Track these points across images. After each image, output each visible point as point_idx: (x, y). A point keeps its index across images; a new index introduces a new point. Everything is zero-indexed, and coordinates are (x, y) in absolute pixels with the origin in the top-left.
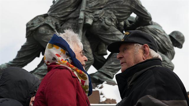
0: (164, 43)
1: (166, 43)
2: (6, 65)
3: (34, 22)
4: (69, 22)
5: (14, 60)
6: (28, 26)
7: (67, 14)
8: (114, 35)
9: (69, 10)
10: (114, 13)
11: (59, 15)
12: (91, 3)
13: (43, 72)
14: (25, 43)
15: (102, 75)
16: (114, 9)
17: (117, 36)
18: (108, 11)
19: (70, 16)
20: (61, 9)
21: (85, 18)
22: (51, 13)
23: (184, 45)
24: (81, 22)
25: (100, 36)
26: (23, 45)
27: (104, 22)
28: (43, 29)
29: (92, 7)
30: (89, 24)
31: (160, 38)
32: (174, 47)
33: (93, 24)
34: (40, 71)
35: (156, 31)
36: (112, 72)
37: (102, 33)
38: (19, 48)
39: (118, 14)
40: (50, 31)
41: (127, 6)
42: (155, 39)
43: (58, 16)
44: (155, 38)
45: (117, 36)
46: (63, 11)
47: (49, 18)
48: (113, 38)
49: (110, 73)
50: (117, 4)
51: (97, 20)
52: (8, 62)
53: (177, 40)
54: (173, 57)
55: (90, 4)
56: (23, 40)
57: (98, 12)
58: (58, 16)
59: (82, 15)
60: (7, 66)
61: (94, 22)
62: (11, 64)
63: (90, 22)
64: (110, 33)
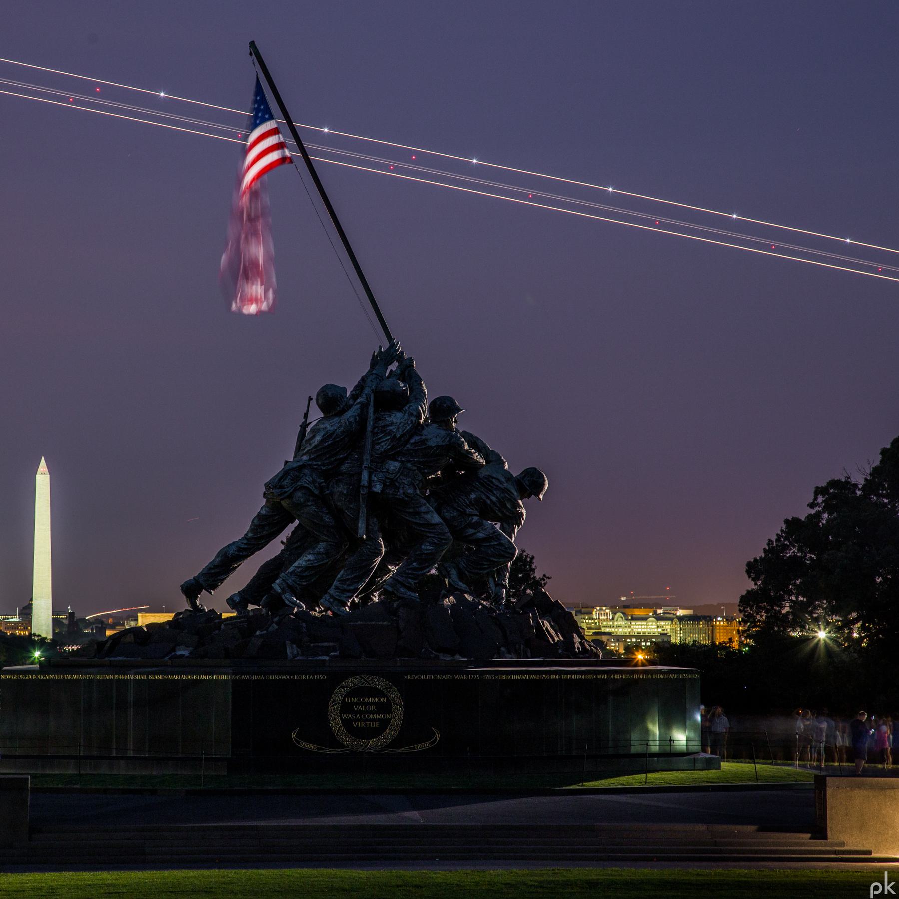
2: (234, 548)
3: (285, 483)
8: (419, 514)
10: (419, 469)
11: (324, 466)
12: (379, 443)
13: (305, 572)
15: (398, 586)
17: (423, 515)
18: (409, 465)
19: (344, 468)
21: (370, 481)
22: (310, 460)
24: (363, 492)
27: (401, 491)
28: (299, 494)
29: (381, 454)
31: (497, 498)
35: (492, 483)
42: (489, 502)
44: (488, 498)
45: (423, 515)
51: (390, 483)
55: (377, 447)
57: (393, 466)
59: (365, 475)
61: (385, 486)
62: (243, 546)
63: (378, 488)
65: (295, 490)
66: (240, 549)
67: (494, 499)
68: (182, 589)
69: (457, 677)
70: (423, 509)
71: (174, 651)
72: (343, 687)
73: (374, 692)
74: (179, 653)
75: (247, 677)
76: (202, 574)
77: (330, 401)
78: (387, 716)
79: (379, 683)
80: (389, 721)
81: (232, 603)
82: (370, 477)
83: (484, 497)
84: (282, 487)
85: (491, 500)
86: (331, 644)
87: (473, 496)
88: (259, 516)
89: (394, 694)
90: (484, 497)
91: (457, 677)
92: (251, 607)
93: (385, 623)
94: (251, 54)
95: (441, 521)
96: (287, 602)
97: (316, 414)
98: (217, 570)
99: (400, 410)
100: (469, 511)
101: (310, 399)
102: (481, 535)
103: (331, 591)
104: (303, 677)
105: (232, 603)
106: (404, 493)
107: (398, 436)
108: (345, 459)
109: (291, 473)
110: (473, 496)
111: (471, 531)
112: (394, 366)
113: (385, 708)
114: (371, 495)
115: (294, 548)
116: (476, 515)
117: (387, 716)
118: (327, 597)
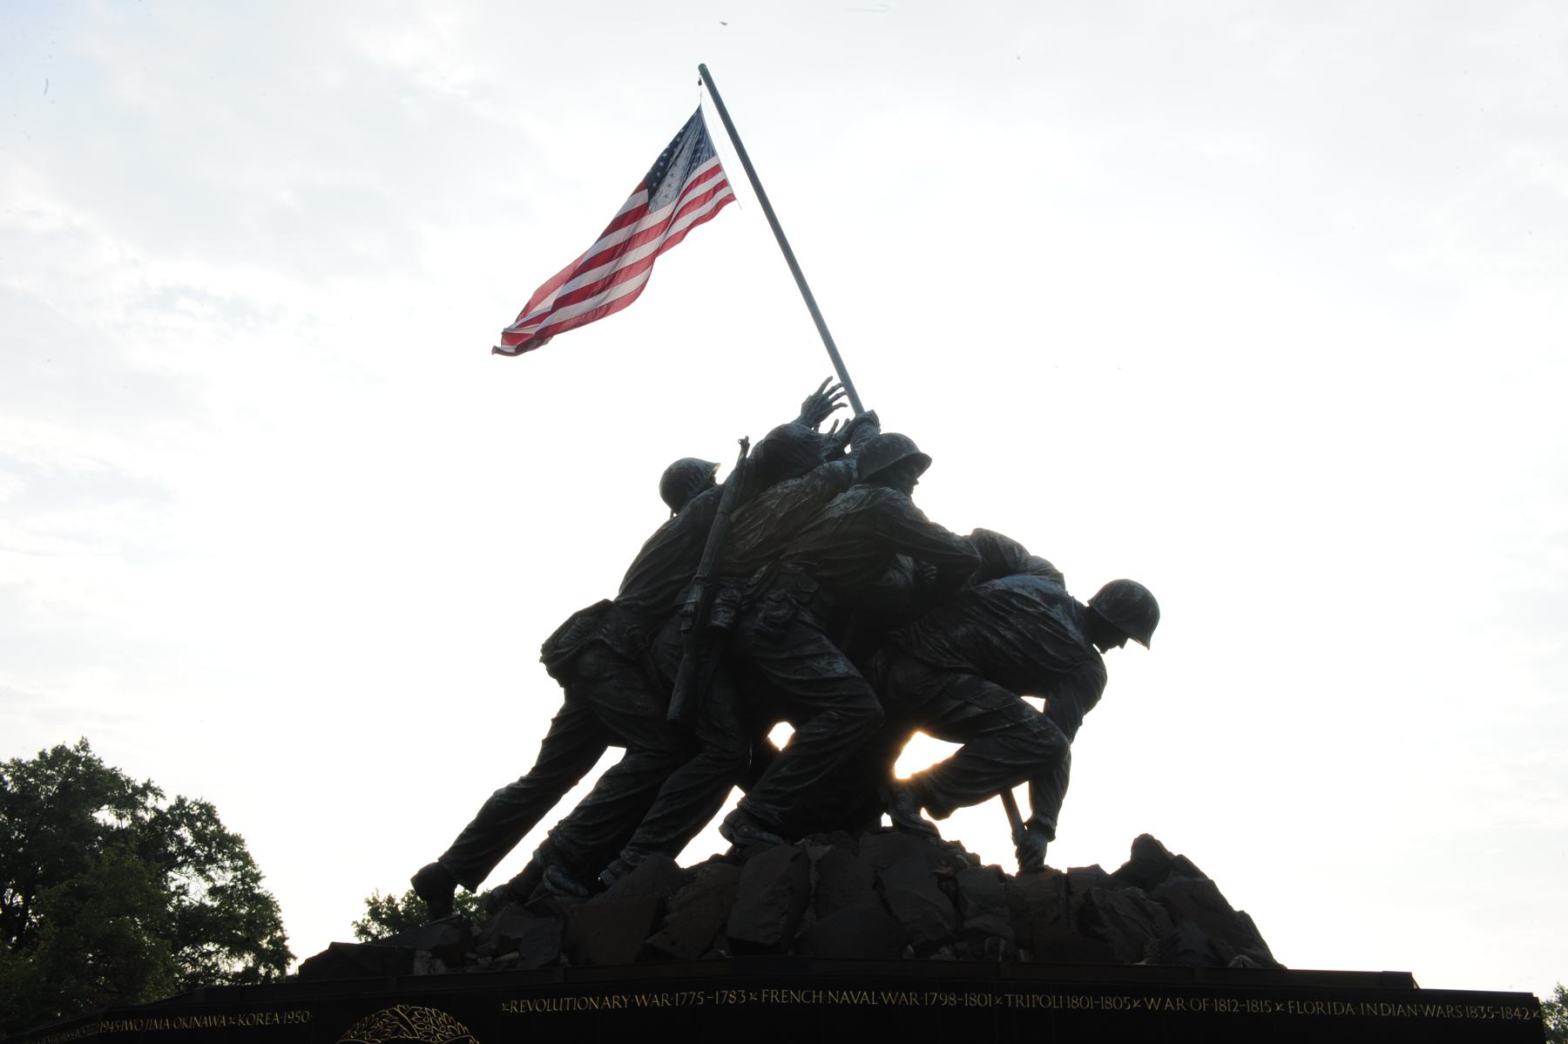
9: (676, 577)
14: (562, 711)
21: (707, 607)
23: (1157, 636)
26: (554, 715)
28: (589, 658)
35: (1010, 604)
38: (544, 729)
42: (995, 641)
43: (642, 603)
44: (996, 633)
49: (768, 806)
52: (515, 780)
53: (1127, 612)
56: (551, 697)
58: (642, 603)
63: (722, 619)
64: (784, 656)
67: (1009, 635)
69: (641, 1000)
70: (811, 649)
83: (985, 632)
84: (557, 648)
85: (1002, 637)
87: (961, 632)
90: (985, 632)
91: (641, 1000)
95: (854, 671)
102: (976, 710)
103: (623, 853)
106: (765, 619)
110: (961, 632)
111: (954, 704)
116: (967, 671)
118: (612, 865)
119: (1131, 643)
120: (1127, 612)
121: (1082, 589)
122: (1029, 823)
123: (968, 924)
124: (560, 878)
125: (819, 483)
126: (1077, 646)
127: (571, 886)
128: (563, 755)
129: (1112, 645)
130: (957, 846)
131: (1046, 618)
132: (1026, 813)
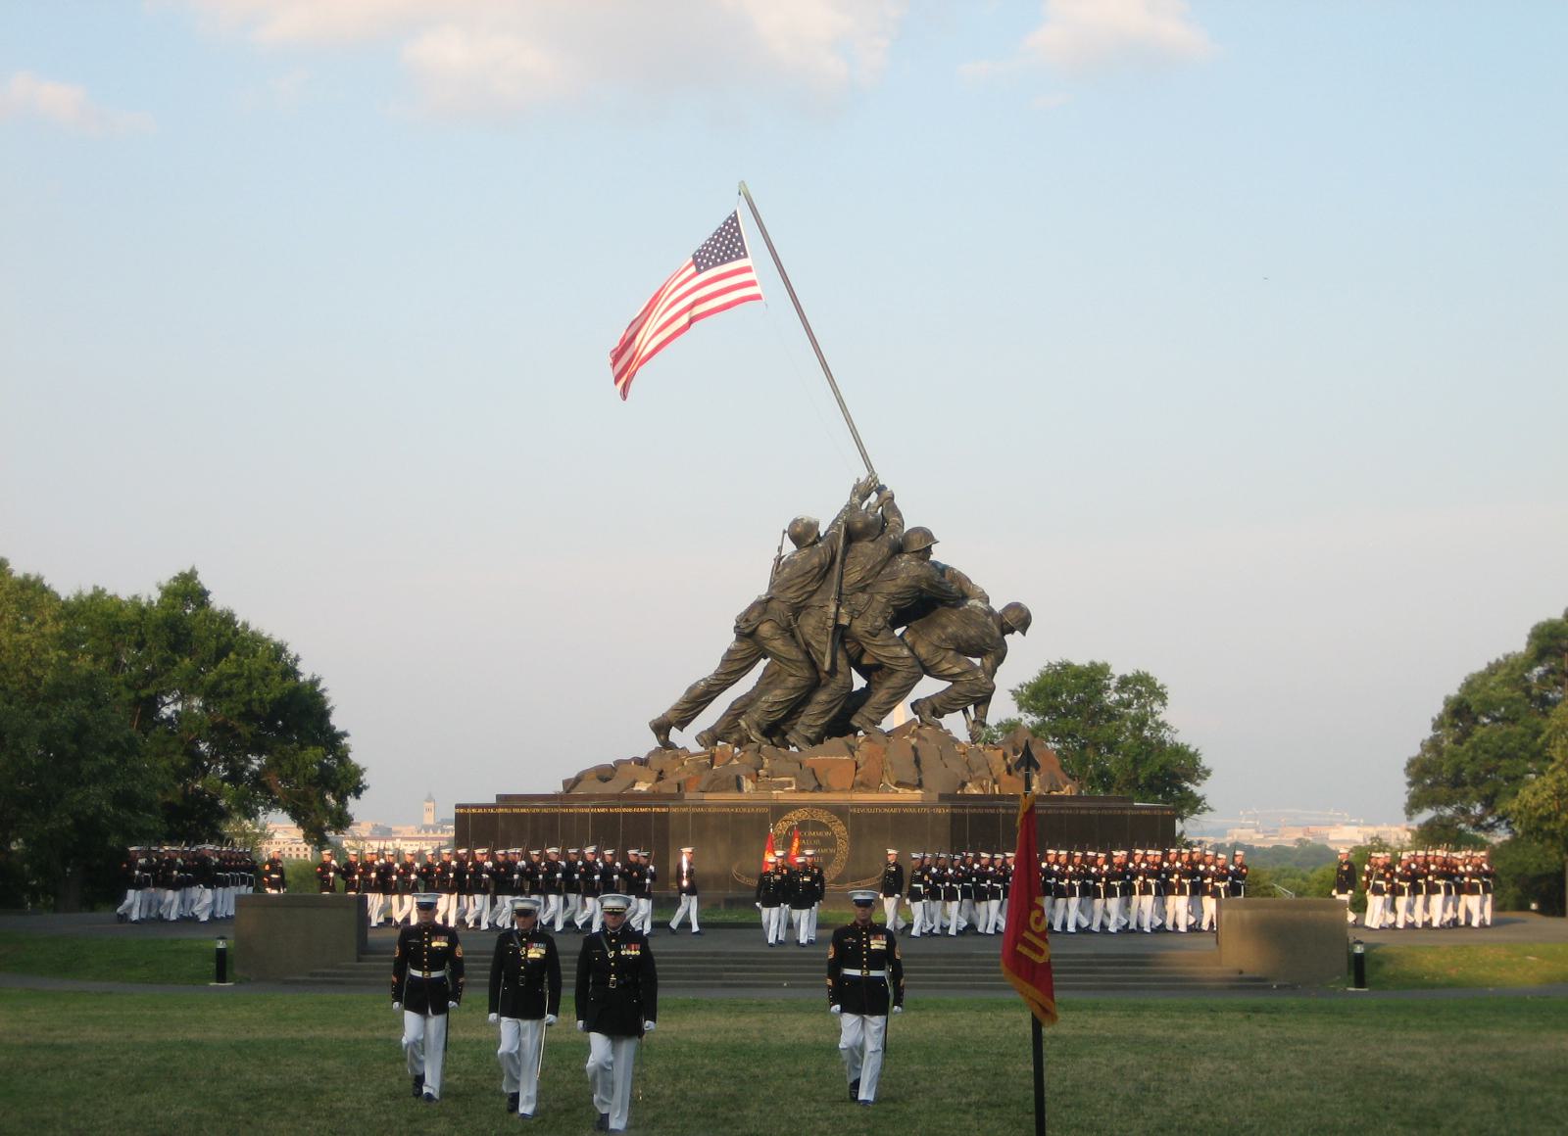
0: (984, 640)
1: (988, 640)
4: (809, 614)
5: (716, 674)
6: (743, 625)
7: (804, 597)
9: (810, 589)
13: (771, 707)
16: (890, 594)
19: (816, 600)
20: (794, 589)
24: (830, 622)
25: (865, 645)
30: (843, 626)
32: (1008, 638)
33: (850, 624)
34: (766, 705)
36: (880, 713)
37: (867, 640)
39: (896, 603)
40: (779, 632)
41: (913, 587)
42: (965, 636)
46: (801, 592)
47: (774, 604)
48: (884, 652)
50: (894, 583)
53: (1018, 619)
54: (1000, 659)
56: (729, 639)
57: (863, 598)
60: (708, 687)
61: (852, 618)
63: (844, 621)
65: (761, 623)
66: (710, 685)
68: (650, 724)
71: (633, 786)
72: (785, 821)
73: (819, 826)
74: (636, 788)
75: (685, 810)
76: (674, 709)
77: (802, 534)
78: (831, 851)
79: (823, 817)
80: (834, 855)
81: (699, 738)
82: (838, 609)
84: (747, 620)
86: (788, 779)
87: (950, 630)
88: (730, 651)
89: (839, 829)
91: (905, 810)
92: (720, 743)
93: (846, 758)
94: (740, 194)
96: (752, 738)
97: (790, 548)
98: (686, 706)
99: (872, 541)
100: (944, 645)
101: (784, 532)
102: (957, 670)
104: (744, 810)
105: (699, 738)
107: (869, 567)
108: (814, 592)
109: (763, 606)
110: (950, 630)
112: (874, 497)
113: (829, 842)
114: (837, 627)
115: (767, 682)
117: (831, 851)
119: (1017, 632)
120: (1018, 619)
121: (998, 605)
122: (974, 722)
123: (977, 774)
124: (759, 736)
125: (886, 550)
126: (998, 639)
127: (764, 739)
128: (733, 668)
129: (1008, 633)
130: (948, 732)
131: (986, 624)
132: (973, 716)
